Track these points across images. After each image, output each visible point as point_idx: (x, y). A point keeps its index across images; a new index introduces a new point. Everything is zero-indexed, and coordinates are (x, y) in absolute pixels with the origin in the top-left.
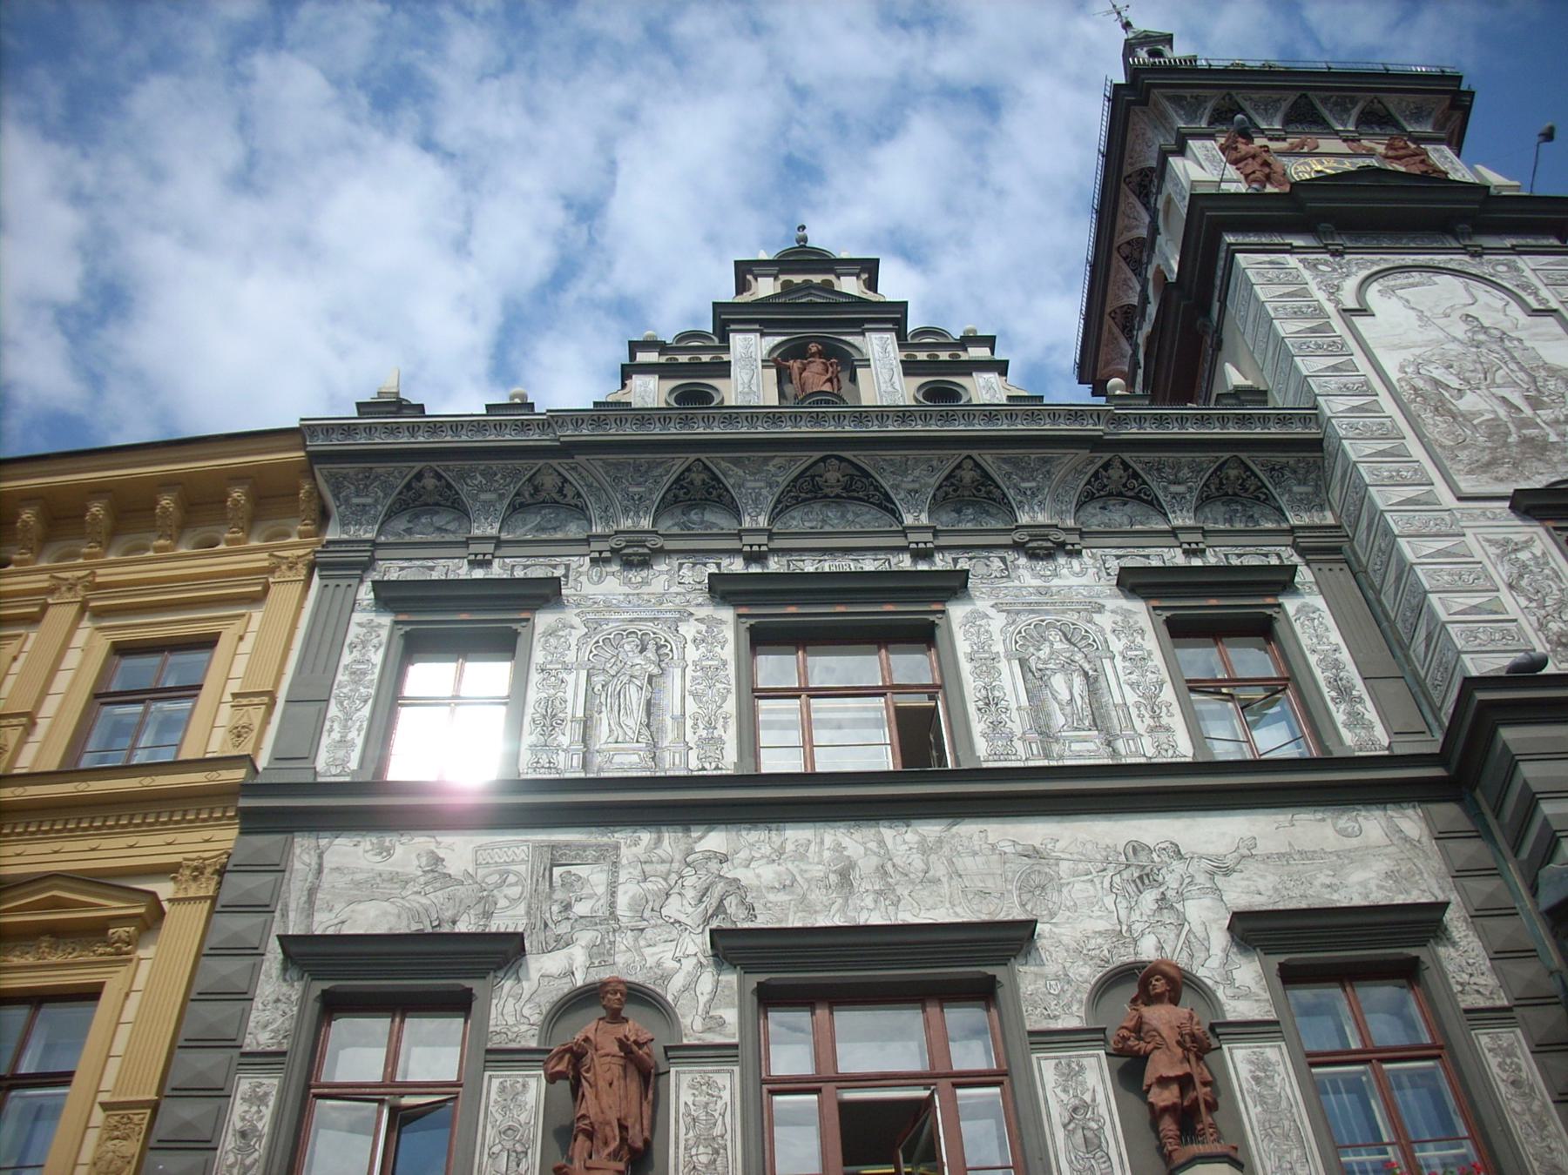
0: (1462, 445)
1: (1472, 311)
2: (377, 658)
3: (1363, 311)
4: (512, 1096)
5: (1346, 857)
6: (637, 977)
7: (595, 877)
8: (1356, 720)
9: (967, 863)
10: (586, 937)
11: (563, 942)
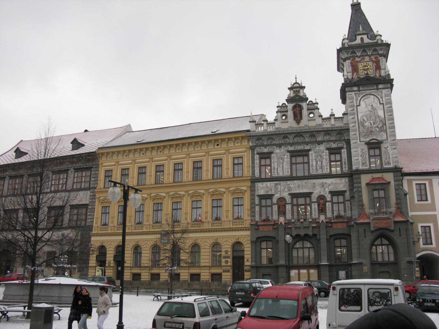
0: (363, 132)
1: (373, 104)
2: (258, 161)
3: (359, 105)
4: (275, 207)
5: (341, 184)
6: (283, 197)
7: (279, 186)
8: (345, 167)
9: (309, 185)
10: (279, 193)
11: (277, 193)
